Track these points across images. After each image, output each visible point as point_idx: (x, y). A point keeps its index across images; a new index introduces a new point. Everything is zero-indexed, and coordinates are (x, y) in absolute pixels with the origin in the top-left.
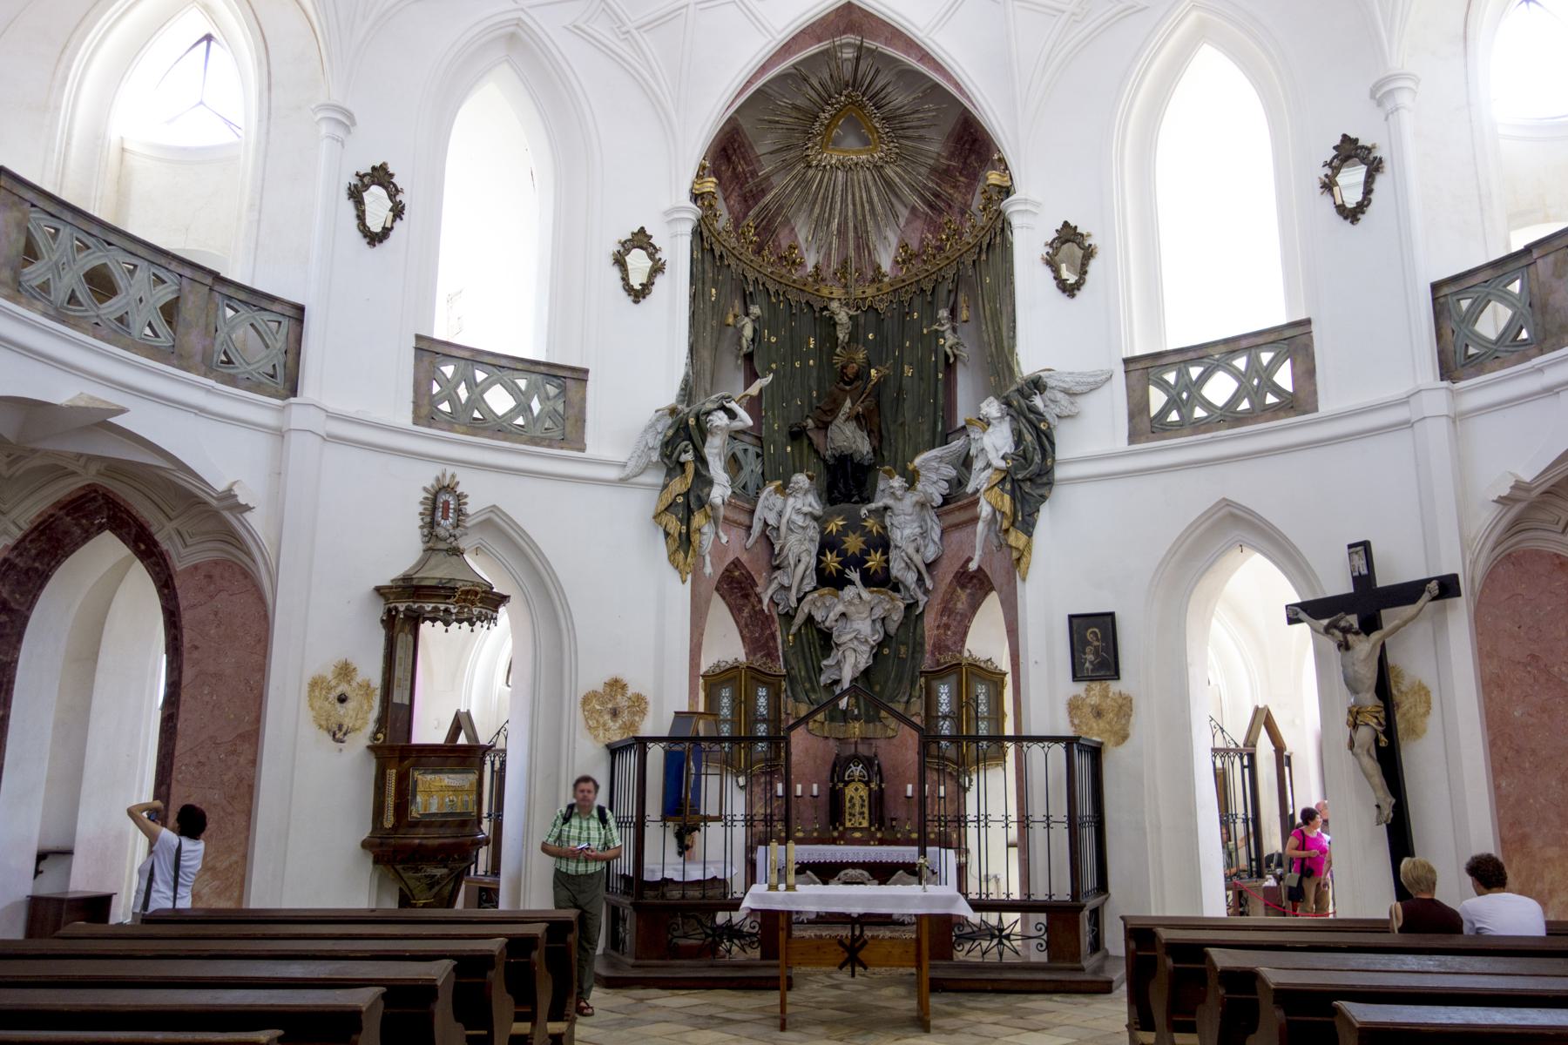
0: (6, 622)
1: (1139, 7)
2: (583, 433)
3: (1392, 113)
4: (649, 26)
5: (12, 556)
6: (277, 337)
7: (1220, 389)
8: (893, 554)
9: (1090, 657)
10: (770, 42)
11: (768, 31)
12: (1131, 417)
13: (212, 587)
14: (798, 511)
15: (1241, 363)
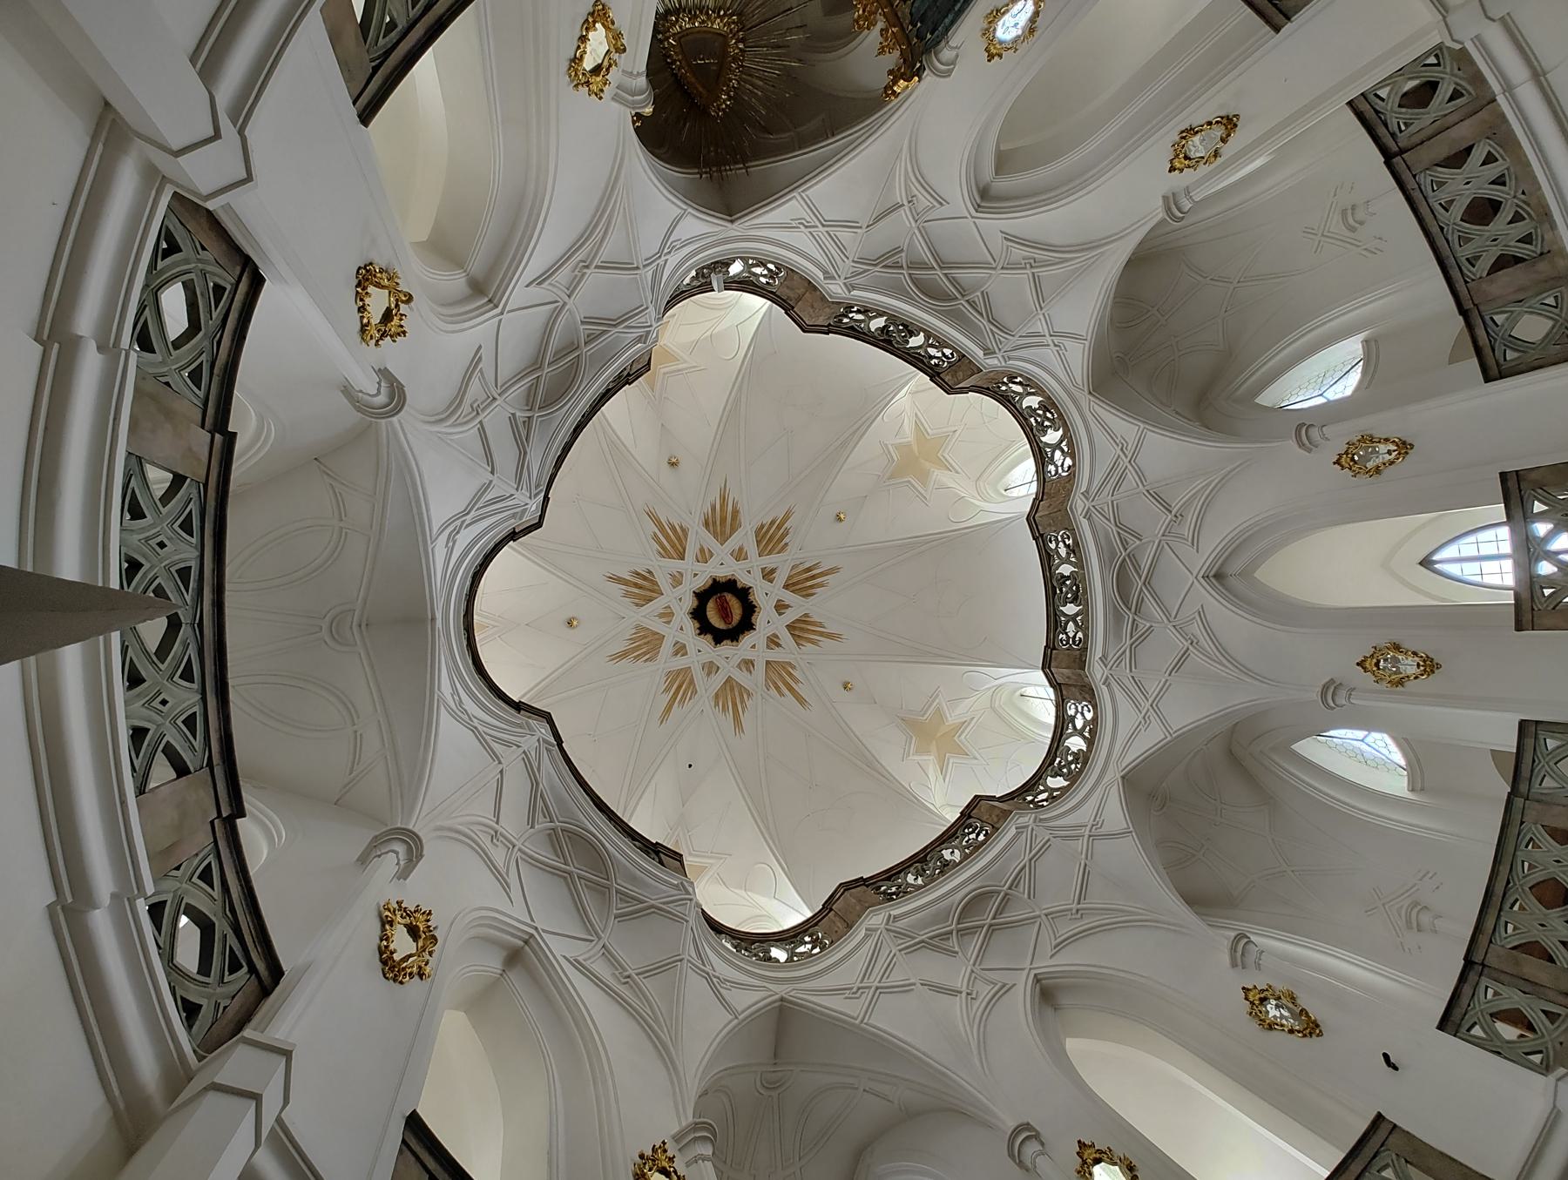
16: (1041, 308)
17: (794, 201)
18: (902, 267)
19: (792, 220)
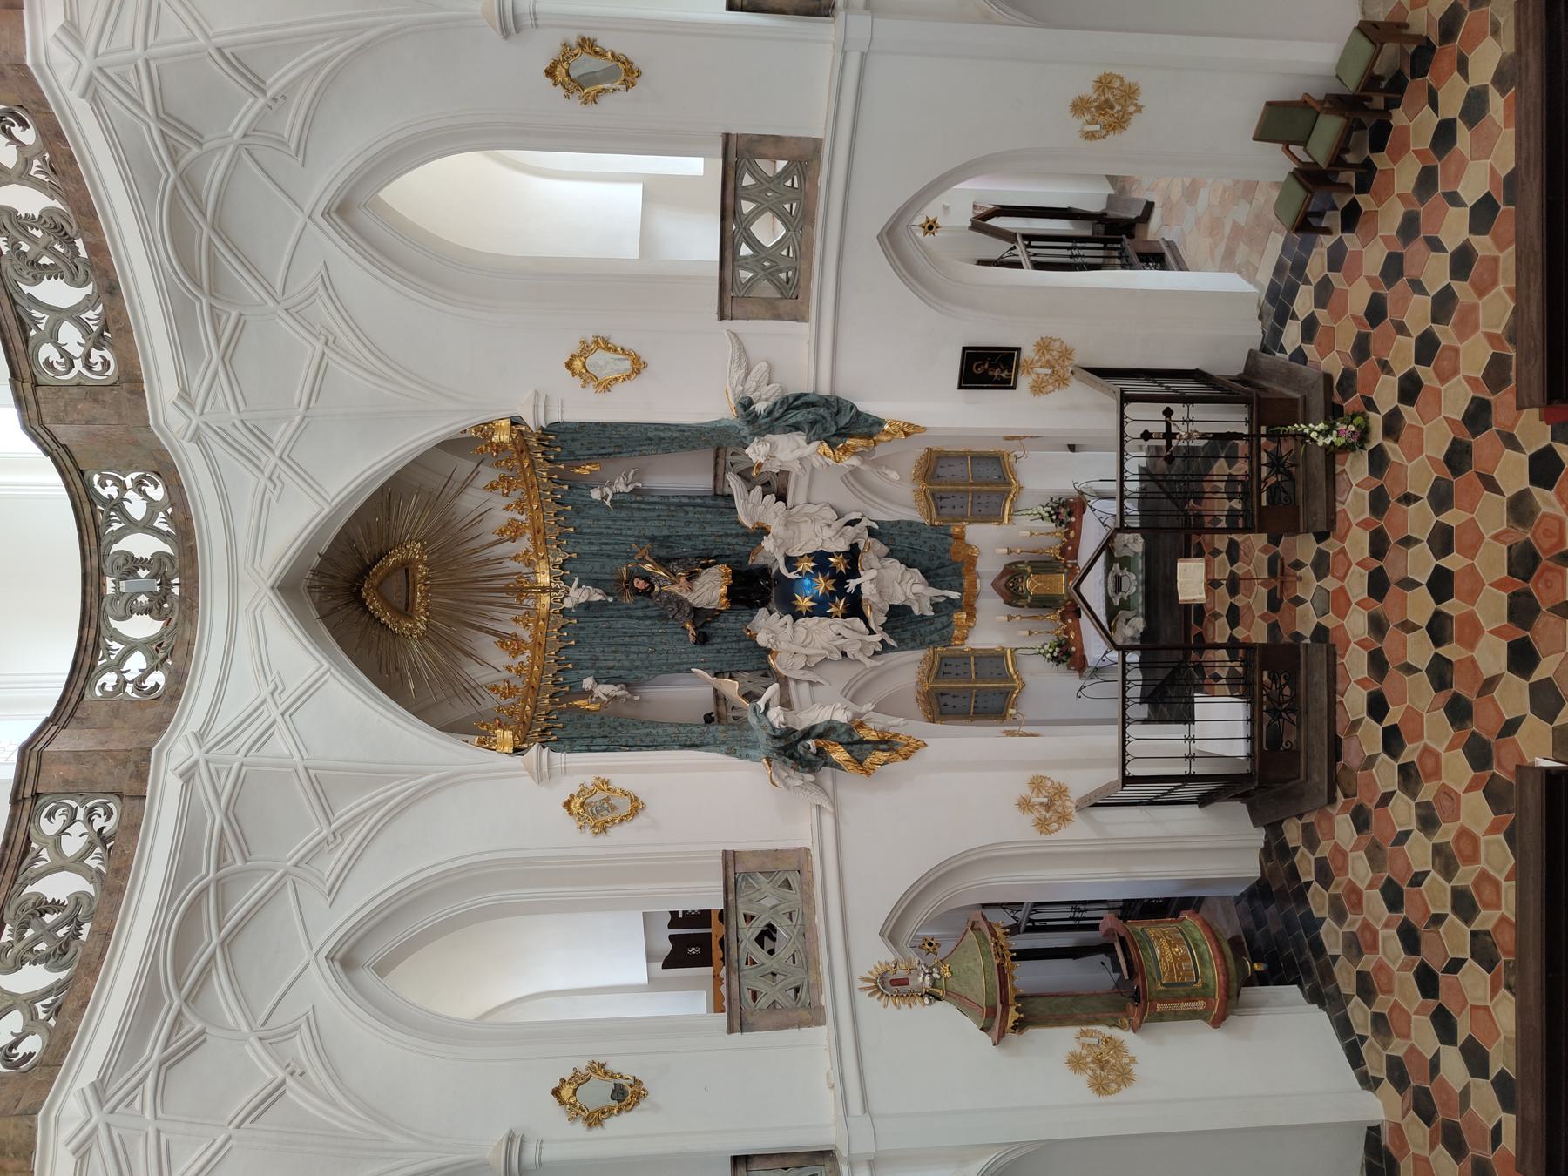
1: (323, 272)
2: (788, 851)
3: (536, 19)
4: (327, 811)
7: (769, 231)
8: (829, 548)
9: (997, 373)
10: (331, 674)
11: (321, 677)
12: (778, 317)
14: (793, 638)
15: (747, 207)
16: (239, 1127)
17: (315, 665)
18: (218, 869)
19: (278, 672)
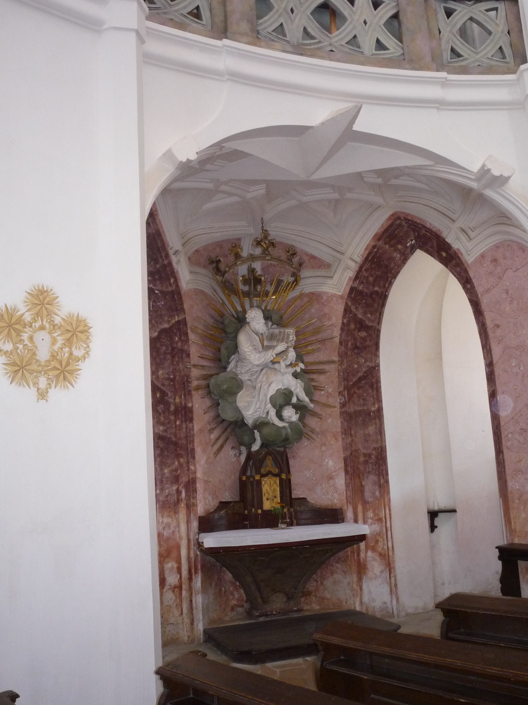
0: (365, 337)
5: (355, 285)
6: (498, 22)
13: (499, 269)
